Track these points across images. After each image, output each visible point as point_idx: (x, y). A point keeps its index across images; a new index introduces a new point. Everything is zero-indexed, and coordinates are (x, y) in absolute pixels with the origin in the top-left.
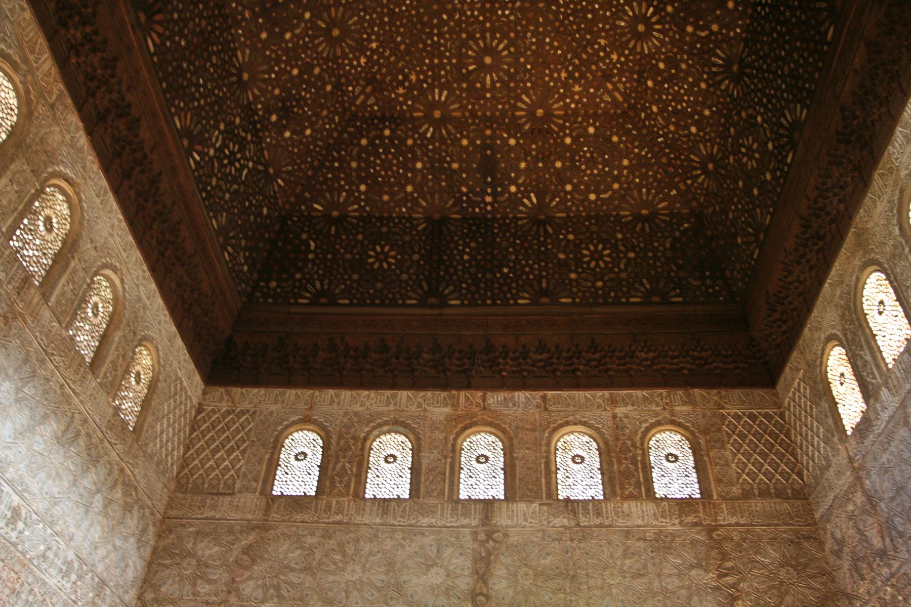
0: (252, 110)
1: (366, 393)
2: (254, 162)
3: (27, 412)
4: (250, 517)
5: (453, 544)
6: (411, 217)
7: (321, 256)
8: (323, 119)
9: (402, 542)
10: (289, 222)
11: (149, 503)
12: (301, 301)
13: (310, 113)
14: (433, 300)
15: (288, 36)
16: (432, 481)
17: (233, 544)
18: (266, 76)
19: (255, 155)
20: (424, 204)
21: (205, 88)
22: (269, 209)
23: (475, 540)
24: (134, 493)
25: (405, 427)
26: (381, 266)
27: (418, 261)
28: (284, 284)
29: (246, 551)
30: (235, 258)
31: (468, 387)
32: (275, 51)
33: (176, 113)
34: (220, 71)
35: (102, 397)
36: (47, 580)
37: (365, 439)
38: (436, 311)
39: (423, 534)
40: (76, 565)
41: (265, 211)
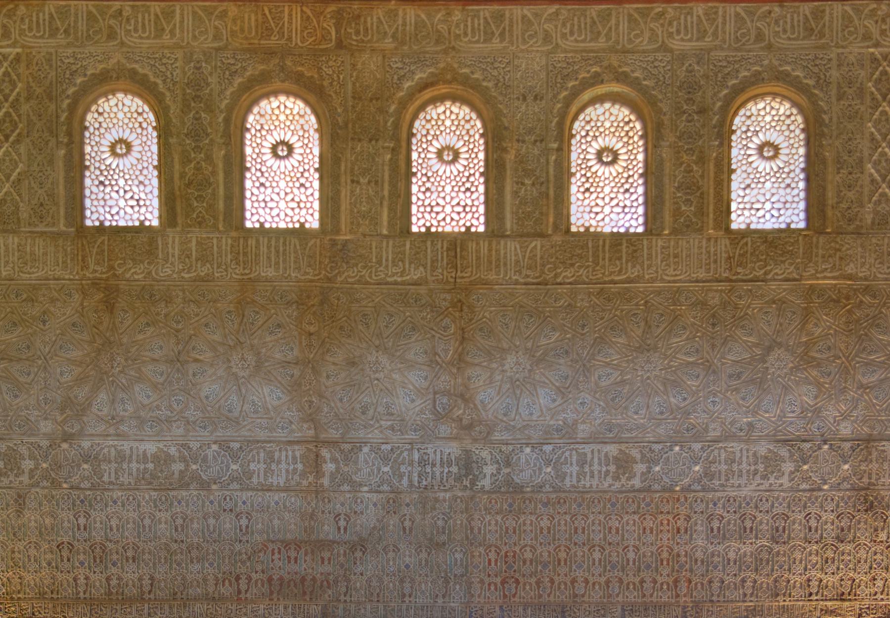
3: (562, 361)
24: (867, 299)
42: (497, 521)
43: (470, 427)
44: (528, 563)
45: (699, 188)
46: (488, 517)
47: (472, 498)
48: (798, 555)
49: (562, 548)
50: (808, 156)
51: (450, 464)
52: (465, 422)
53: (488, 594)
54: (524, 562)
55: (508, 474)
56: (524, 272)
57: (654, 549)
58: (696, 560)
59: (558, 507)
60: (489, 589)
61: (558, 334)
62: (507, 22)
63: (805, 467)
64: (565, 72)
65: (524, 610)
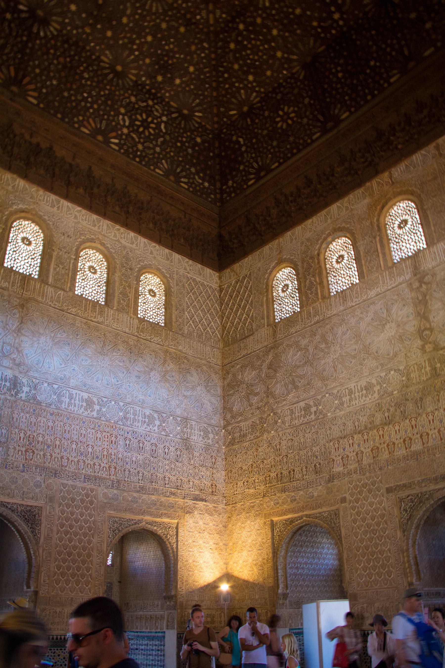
0: (140, 85)
1: (310, 221)
2: (166, 116)
3: (66, 348)
4: (266, 344)
5: (396, 301)
6: (293, 74)
7: (249, 144)
8: (195, 52)
9: (361, 316)
10: (223, 136)
11: (203, 362)
12: (250, 183)
13: (182, 56)
14: (330, 125)
15: (125, 20)
16: (370, 260)
17: (262, 365)
18: (132, 57)
19: (163, 111)
20: (295, 57)
21: (92, 97)
22: (201, 137)
23: (412, 289)
24: (186, 361)
25: (341, 231)
26: (288, 124)
27: (310, 103)
28: (236, 179)
29: (270, 367)
30: (193, 183)
31: (377, 173)
32: (125, 37)
33: (80, 126)
34: (96, 79)
35: (124, 317)
36: (135, 430)
37: (318, 255)
38: (335, 131)
39: (374, 303)
40: (156, 415)
41: (199, 140)
42: (26, 417)
43: (19, 365)
44: (40, 443)
45: (128, 296)
46: (22, 414)
47: (15, 402)
48: (160, 464)
49: (58, 439)
50: (166, 300)
51: (6, 381)
52: (17, 362)
53: (17, 456)
54: (38, 443)
55: (35, 394)
56: (54, 303)
57: (101, 449)
58: (119, 458)
59: (58, 417)
60: (18, 453)
61: (66, 335)
62: (61, 205)
63: (164, 425)
64: (82, 232)
65: (36, 469)
